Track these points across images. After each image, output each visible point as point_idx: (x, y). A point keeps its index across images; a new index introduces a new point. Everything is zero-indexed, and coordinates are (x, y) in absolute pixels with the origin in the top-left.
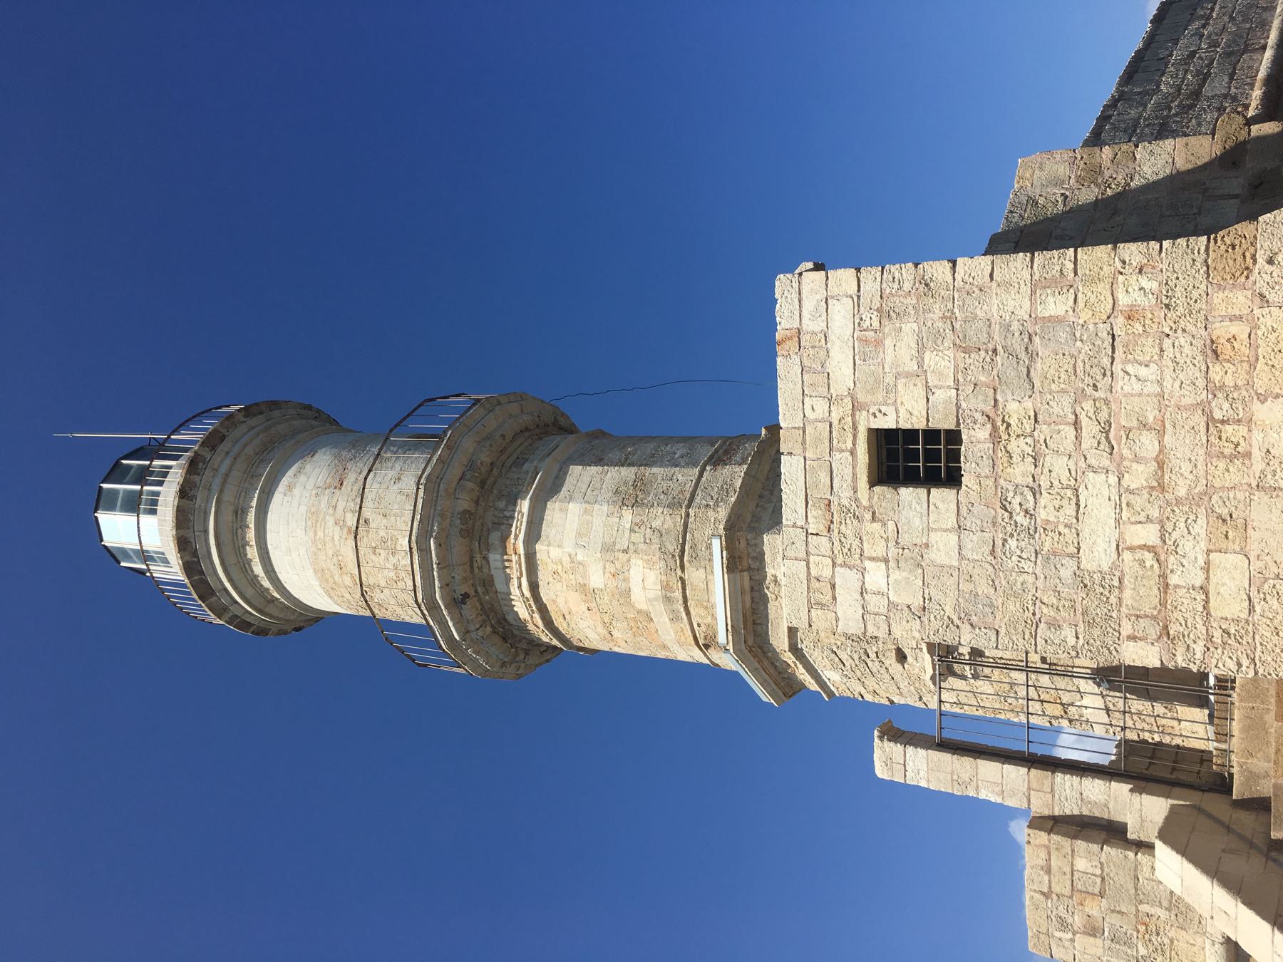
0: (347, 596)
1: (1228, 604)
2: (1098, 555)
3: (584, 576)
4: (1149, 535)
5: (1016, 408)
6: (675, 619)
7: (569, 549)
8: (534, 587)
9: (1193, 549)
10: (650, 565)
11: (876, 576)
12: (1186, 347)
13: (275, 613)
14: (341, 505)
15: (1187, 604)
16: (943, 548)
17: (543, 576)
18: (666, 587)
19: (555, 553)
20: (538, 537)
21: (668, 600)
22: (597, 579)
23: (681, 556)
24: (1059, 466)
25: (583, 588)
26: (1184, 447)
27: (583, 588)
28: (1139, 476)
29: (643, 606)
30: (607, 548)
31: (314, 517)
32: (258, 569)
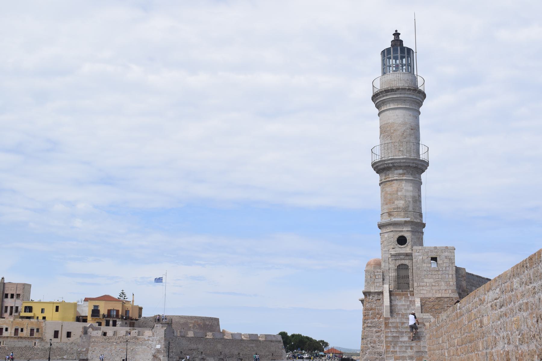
0: (388, 129)
1: (422, 292)
2: (425, 280)
3: (400, 191)
4: (428, 285)
5: (440, 273)
6: (394, 209)
7: (405, 188)
8: (396, 180)
9: (427, 289)
10: (403, 205)
11: (421, 257)
12: (446, 288)
13: (380, 102)
14: (408, 131)
15: (421, 288)
16: (425, 265)
17: (399, 182)
18: (399, 208)
19: (403, 185)
20: (406, 182)
21: (397, 208)
22: (399, 194)
23: (405, 210)
24: (434, 277)
25: (397, 191)
26: (437, 288)
27: (397, 191)
28: (434, 284)
29: (396, 202)
30: (405, 196)
31: (405, 124)
32: (392, 106)
